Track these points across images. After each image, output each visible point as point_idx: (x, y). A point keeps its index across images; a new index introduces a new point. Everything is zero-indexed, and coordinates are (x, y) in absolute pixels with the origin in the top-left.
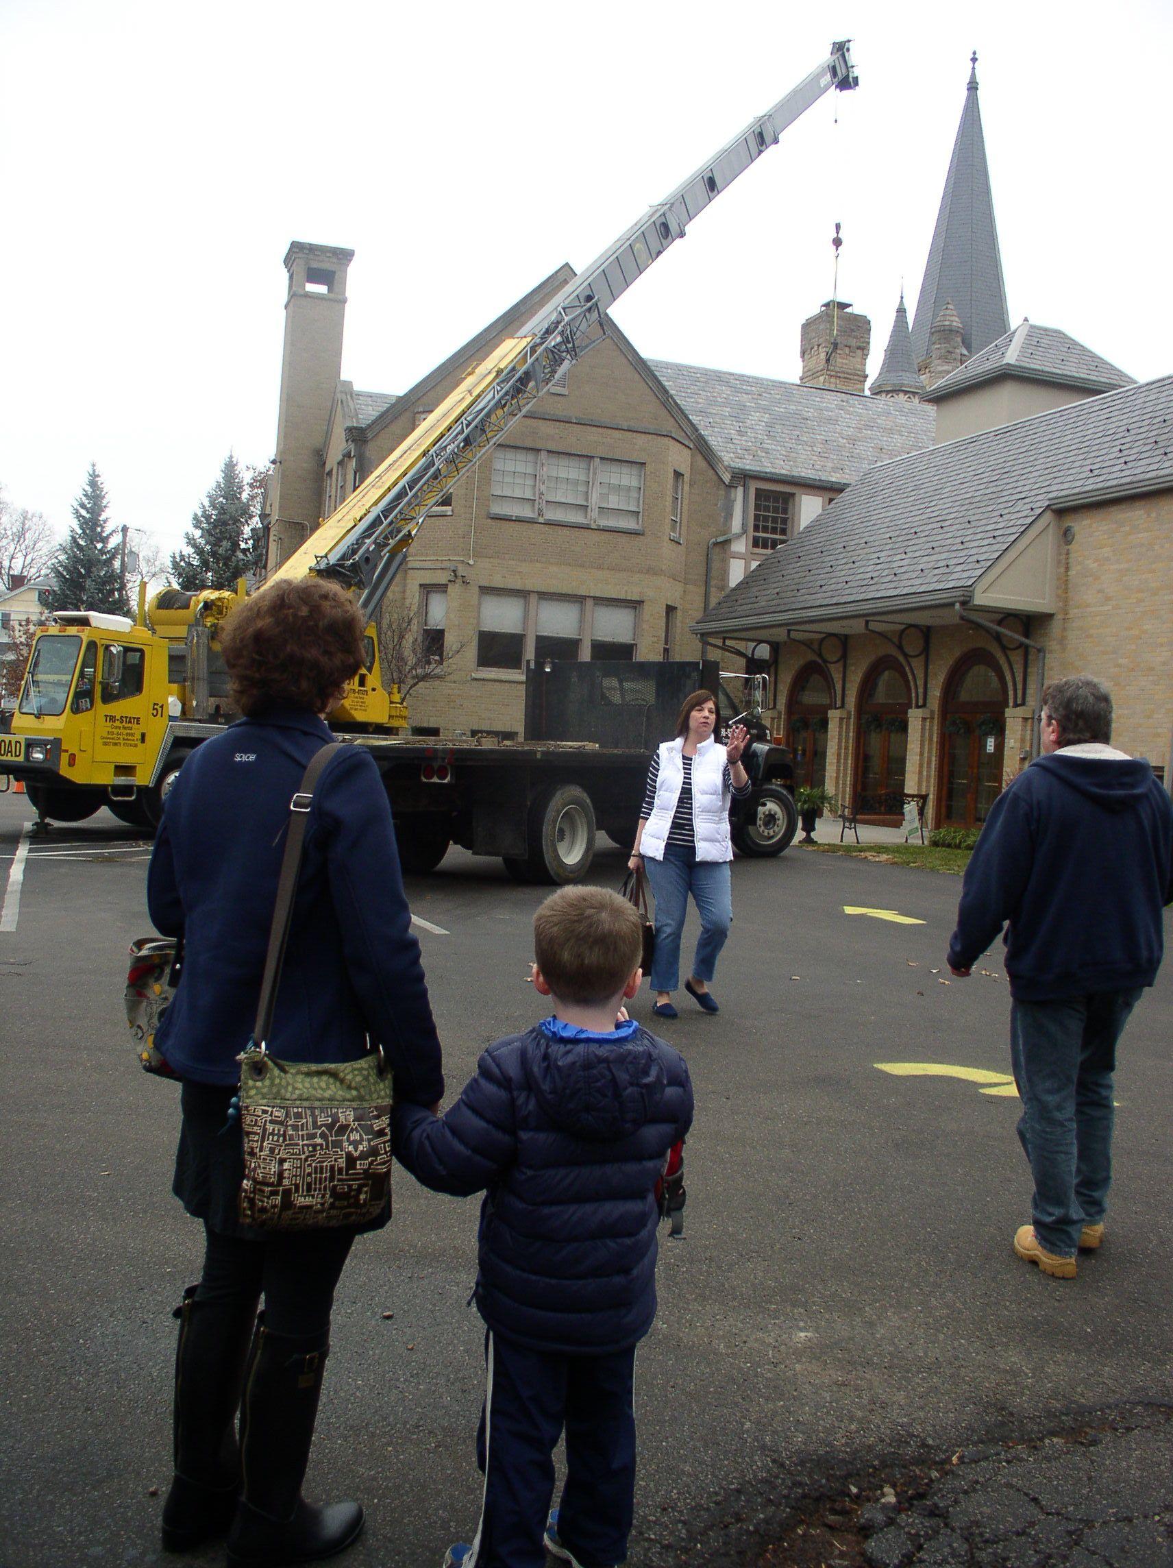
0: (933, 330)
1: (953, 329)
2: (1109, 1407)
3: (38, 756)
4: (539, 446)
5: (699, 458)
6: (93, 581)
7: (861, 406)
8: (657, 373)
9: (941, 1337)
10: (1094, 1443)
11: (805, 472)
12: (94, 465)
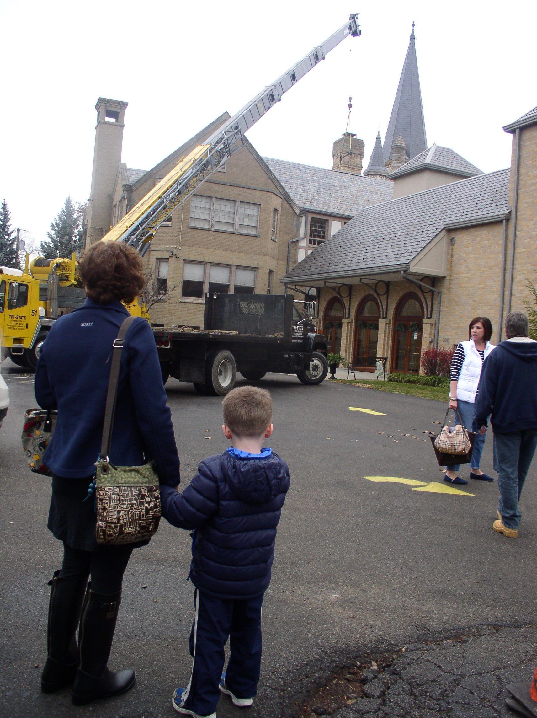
2: (472, 627)
4: (212, 195)
5: (285, 203)
6: (4, 253)
8: (267, 163)
9: (397, 597)
10: (465, 642)
11: (333, 210)
12: (4, 200)
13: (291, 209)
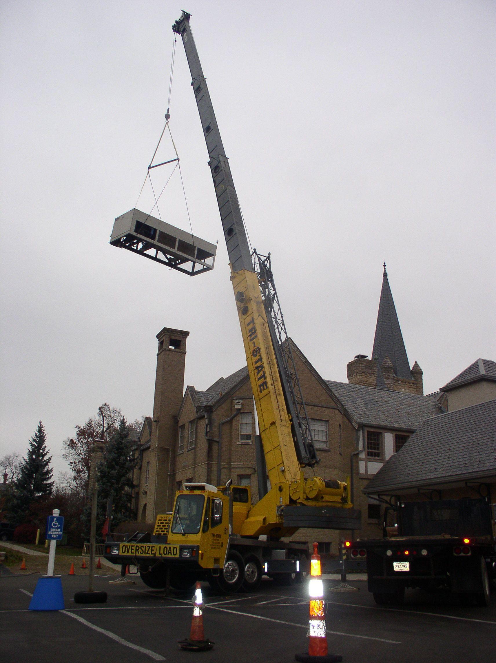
0: (382, 367)
1: (390, 367)
3: (187, 554)
6: (39, 474)
7: (395, 396)
13: (350, 424)
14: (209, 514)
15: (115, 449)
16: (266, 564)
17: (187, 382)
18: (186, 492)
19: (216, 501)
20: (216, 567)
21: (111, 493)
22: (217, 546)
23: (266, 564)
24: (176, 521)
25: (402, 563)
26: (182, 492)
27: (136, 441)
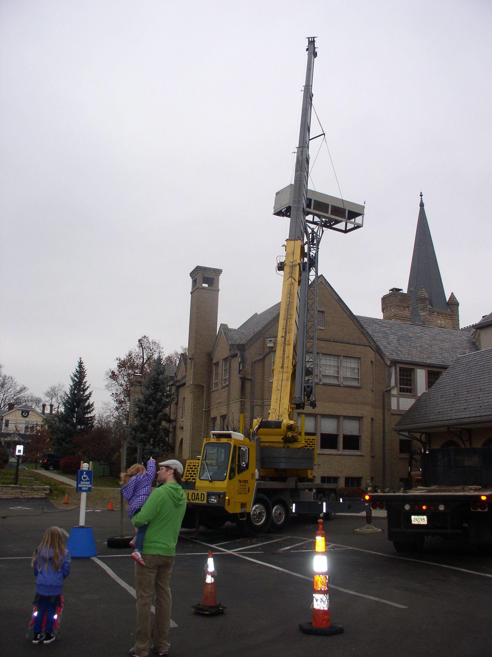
3: (214, 500)
5: (377, 355)
11: (417, 360)
13: (382, 361)
14: (236, 462)
15: (152, 385)
16: (294, 505)
17: (220, 321)
18: (213, 440)
19: (242, 448)
20: (242, 511)
21: (149, 428)
22: (244, 491)
23: (294, 505)
24: (204, 469)
25: (420, 516)
26: (210, 440)
27: (173, 376)
